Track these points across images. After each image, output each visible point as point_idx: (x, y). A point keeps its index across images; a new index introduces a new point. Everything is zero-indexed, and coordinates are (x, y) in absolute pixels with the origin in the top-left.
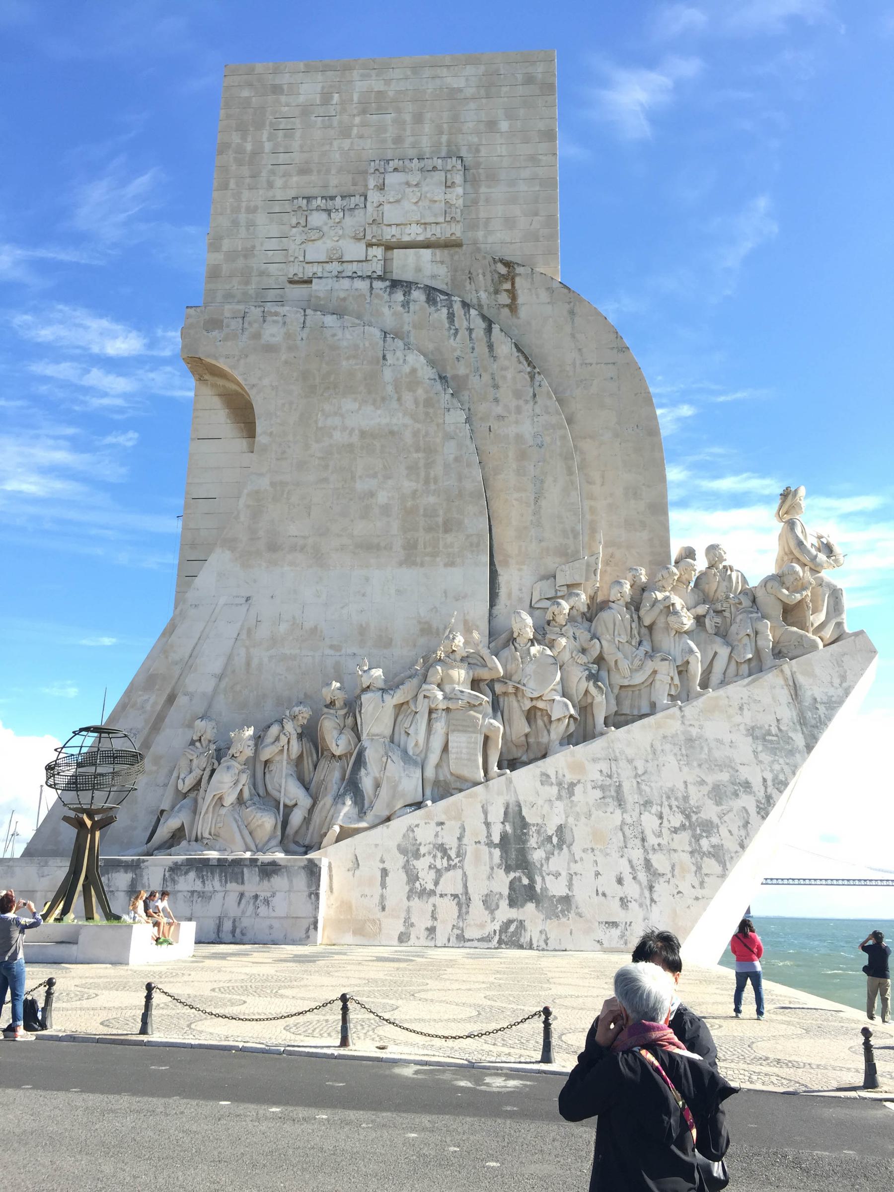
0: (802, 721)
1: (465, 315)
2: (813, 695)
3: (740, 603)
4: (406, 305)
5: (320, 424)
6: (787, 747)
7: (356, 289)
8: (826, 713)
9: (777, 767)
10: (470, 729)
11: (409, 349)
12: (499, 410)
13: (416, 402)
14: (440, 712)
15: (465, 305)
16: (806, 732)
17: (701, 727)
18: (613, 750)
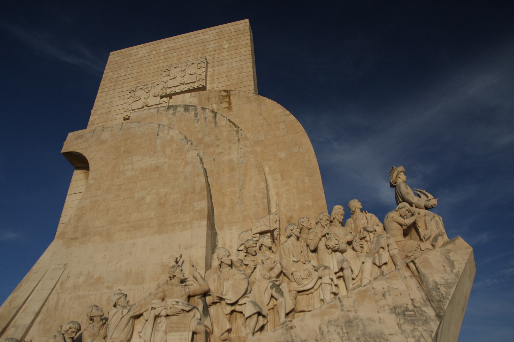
0: (429, 299)
1: (203, 112)
2: (434, 280)
3: (376, 231)
4: (174, 114)
5: (121, 170)
6: (421, 318)
7: (151, 113)
8: (445, 290)
9: (417, 334)
10: (183, 329)
11: (171, 129)
12: (219, 150)
13: (172, 151)
14: (162, 318)
15: (203, 109)
16: (434, 306)
17: (356, 311)
18: (291, 336)
